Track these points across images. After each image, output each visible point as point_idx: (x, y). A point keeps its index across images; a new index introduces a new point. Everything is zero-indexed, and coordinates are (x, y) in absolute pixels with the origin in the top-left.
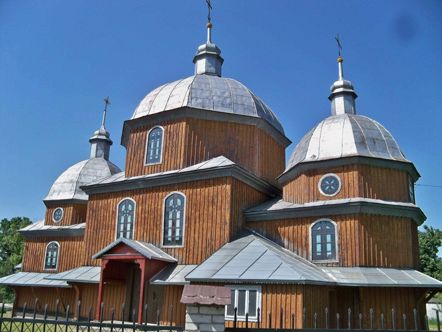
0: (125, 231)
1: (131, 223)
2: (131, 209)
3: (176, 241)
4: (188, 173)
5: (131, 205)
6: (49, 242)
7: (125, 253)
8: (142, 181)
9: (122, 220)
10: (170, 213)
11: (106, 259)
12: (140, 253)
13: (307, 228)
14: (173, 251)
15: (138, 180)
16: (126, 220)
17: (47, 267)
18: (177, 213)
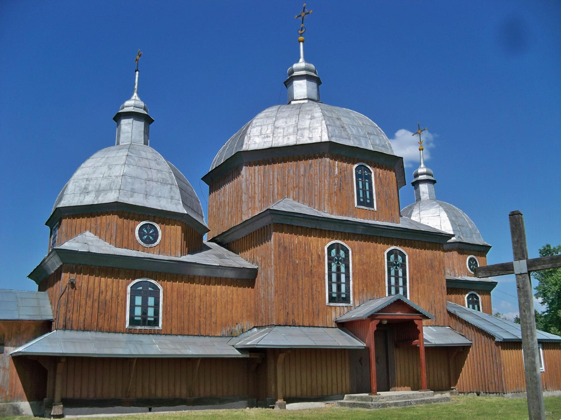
0: (340, 283)
1: (345, 274)
2: (344, 256)
3: (343, 298)
4: (418, 231)
5: (343, 250)
6: (134, 279)
7: (395, 313)
8: (364, 226)
9: (391, 272)
10: (332, 265)
11: (377, 319)
12: (421, 313)
13: (464, 298)
14: (338, 309)
15: (363, 224)
16: (338, 269)
17: (133, 322)
18: (399, 271)
